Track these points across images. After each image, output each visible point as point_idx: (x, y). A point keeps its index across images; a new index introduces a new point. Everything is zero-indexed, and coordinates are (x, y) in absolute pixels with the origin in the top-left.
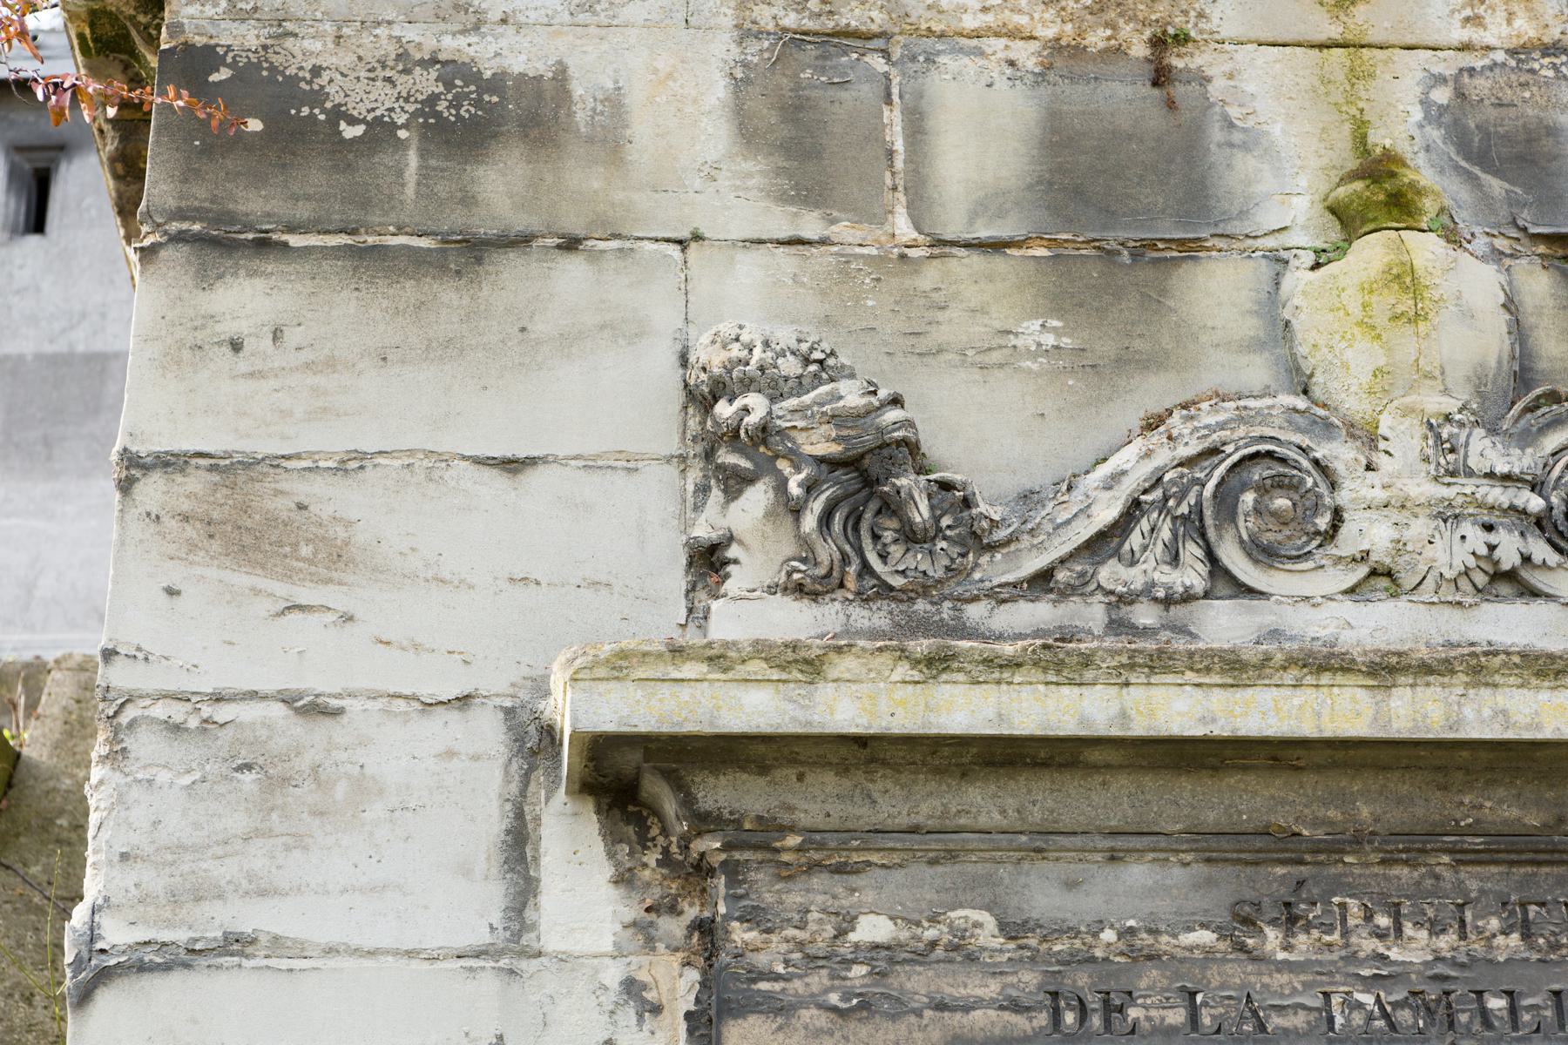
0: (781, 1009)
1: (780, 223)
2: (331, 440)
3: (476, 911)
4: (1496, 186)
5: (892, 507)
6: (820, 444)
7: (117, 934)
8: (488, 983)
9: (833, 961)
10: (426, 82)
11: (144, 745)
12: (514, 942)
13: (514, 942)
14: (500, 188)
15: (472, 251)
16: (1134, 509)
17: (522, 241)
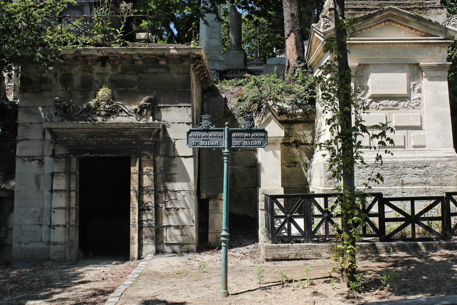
0: (59, 143)
1: (62, 89)
2: (32, 105)
3: (42, 137)
4: (113, 84)
5: (67, 111)
6: (62, 107)
7: (19, 138)
8: (42, 142)
9: (62, 140)
10: (38, 78)
11: (21, 126)
12: (44, 139)
13: (44, 139)
14: (43, 86)
15: (41, 91)
16: (83, 111)
17: (45, 90)
